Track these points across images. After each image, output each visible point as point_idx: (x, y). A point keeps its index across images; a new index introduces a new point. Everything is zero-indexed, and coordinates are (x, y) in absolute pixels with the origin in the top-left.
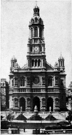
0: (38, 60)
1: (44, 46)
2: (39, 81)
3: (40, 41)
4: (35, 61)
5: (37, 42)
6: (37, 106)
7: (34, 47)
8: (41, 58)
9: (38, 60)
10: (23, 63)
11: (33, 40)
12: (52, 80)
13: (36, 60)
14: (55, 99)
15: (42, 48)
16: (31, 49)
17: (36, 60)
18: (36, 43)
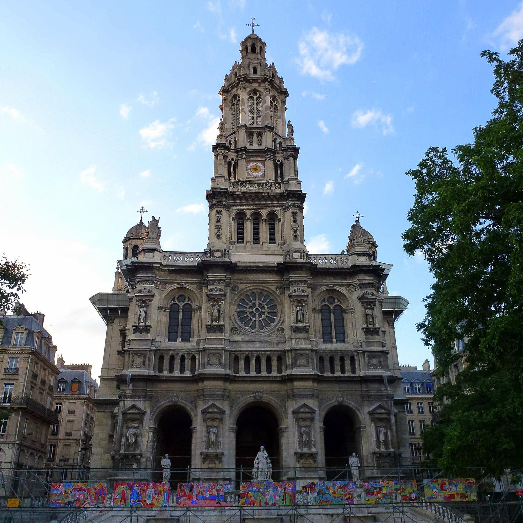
0: (264, 213)
1: (295, 158)
2: (275, 314)
3: (275, 141)
4: (248, 216)
5: (260, 144)
6: (266, 448)
7: (248, 162)
8: (281, 206)
9: (264, 213)
10: (188, 231)
11: (242, 135)
12: (340, 312)
13: (257, 217)
14: (370, 413)
15: (282, 165)
16: (232, 167)
17: (257, 216)
18: (255, 146)
